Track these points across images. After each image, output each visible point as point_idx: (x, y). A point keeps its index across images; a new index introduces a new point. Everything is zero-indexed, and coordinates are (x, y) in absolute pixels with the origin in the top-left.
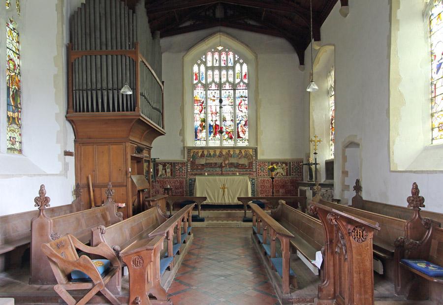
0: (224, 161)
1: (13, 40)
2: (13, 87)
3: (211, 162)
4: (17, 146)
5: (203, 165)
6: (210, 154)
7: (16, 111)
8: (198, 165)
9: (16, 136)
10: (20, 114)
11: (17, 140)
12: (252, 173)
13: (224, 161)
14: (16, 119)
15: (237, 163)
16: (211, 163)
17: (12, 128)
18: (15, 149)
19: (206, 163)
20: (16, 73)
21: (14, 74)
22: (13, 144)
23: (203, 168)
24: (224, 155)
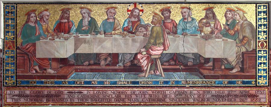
0: (147, 48)
3: (96, 50)
5: (63, 61)
6: (92, 22)
8: (44, 63)
12: (253, 91)
13: (147, 48)
15: (197, 56)
16: (98, 55)
19: (76, 56)
23: (62, 72)
24: (146, 27)
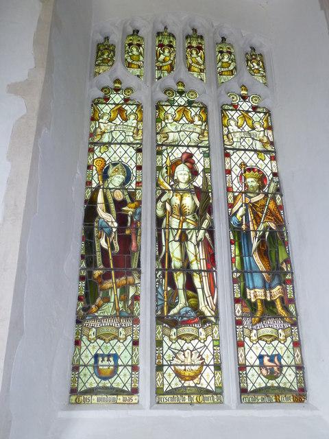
1: (253, 129)
2: (262, 227)
4: (289, 378)
7: (276, 281)
9: (281, 349)
10: (289, 288)
11: (286, 360)
14: (278, 303)
17: (268, 331)
18: (280, 391)
20: (266, 195)
21: (261, 196)
22: (272, 375)
